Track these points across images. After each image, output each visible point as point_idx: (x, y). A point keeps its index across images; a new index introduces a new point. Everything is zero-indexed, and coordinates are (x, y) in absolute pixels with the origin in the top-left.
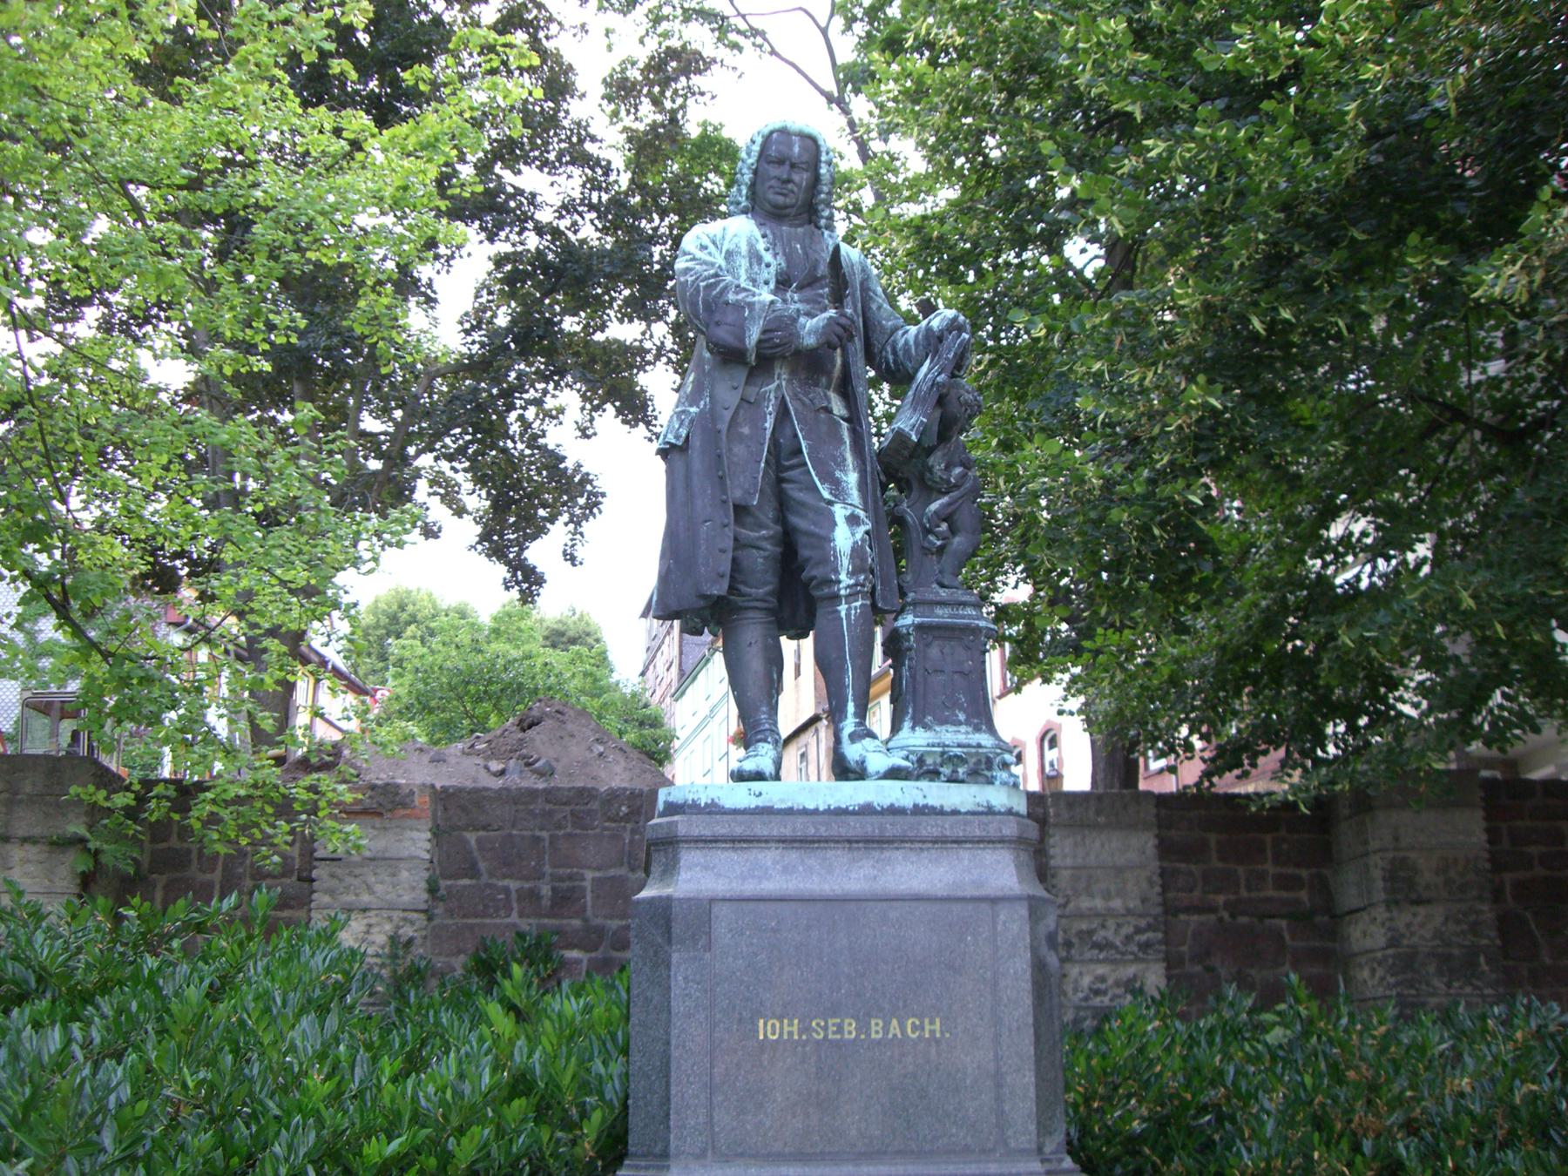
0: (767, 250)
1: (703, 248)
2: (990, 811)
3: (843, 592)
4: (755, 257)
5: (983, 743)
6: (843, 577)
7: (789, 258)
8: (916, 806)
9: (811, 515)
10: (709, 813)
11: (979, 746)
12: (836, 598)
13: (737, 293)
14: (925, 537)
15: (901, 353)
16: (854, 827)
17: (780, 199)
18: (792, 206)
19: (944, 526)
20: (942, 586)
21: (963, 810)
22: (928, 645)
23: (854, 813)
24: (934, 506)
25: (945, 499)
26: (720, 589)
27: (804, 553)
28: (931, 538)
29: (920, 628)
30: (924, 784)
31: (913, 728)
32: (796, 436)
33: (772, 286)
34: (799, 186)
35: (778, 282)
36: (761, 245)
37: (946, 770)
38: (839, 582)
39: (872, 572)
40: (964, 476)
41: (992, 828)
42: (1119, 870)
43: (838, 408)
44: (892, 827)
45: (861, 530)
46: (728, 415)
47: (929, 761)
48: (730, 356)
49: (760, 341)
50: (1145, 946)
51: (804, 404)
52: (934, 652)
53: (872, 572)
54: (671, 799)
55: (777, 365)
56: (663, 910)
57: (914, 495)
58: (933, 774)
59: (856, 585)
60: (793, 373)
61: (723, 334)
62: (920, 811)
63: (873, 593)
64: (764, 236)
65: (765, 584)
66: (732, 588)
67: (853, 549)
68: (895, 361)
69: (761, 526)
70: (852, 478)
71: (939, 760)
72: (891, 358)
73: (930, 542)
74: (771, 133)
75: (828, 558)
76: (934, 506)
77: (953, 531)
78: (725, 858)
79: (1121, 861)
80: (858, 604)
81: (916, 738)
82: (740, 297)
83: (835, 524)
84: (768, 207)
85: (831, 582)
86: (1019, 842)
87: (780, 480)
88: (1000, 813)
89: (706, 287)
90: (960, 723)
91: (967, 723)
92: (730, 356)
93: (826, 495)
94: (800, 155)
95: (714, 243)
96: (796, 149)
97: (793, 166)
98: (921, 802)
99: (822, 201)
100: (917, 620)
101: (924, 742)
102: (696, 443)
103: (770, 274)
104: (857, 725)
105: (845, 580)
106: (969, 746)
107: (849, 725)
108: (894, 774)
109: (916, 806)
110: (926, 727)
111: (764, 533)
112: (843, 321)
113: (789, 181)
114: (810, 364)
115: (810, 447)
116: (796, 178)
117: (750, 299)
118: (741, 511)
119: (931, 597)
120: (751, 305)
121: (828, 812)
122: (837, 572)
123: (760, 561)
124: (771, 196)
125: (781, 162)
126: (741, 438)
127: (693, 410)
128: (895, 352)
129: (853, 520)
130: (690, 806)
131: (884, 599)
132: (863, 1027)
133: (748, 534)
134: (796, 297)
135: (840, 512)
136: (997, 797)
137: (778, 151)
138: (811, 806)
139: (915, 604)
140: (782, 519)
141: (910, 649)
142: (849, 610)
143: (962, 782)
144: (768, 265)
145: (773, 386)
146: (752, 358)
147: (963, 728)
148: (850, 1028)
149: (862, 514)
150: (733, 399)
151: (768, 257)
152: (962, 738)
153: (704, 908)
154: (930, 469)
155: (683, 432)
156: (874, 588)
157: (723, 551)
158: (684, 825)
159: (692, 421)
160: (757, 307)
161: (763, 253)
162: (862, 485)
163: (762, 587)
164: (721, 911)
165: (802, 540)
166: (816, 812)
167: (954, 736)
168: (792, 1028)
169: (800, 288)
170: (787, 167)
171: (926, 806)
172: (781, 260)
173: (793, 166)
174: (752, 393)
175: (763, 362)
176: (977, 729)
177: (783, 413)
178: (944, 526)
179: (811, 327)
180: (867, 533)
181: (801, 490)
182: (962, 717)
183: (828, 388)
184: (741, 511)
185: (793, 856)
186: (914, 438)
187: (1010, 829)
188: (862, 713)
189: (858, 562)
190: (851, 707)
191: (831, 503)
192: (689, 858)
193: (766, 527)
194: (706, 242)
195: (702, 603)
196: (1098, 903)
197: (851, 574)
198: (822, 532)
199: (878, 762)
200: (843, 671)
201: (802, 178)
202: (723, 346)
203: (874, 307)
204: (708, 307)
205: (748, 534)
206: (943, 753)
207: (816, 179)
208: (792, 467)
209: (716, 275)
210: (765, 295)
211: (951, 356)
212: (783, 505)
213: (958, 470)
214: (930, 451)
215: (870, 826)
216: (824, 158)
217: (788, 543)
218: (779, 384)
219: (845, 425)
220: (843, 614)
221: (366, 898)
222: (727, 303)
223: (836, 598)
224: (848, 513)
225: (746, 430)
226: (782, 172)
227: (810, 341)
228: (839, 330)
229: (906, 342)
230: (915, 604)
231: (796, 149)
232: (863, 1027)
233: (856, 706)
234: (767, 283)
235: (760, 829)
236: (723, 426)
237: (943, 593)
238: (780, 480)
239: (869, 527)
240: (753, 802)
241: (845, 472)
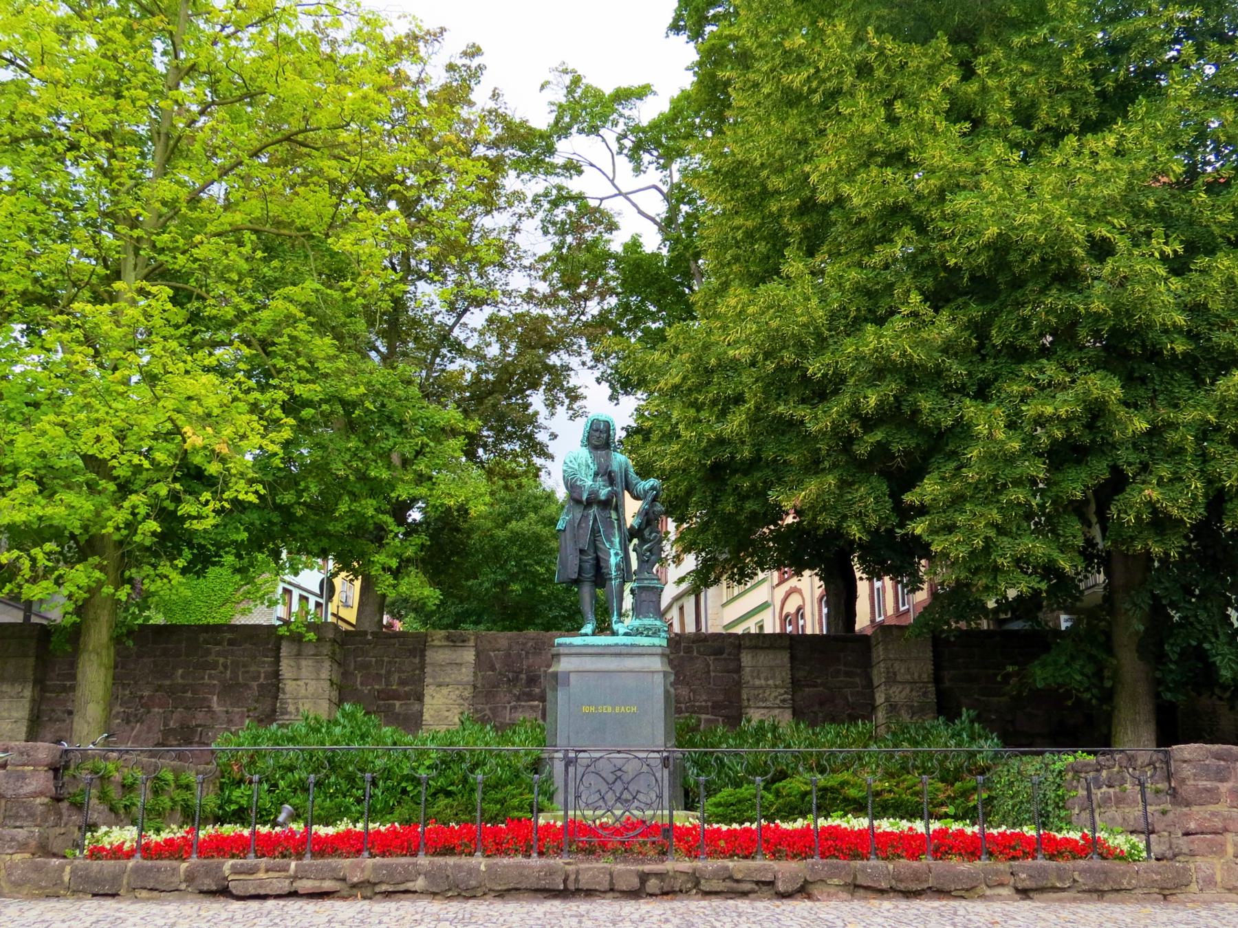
2: (654, 646)
16: (612, 650)
26: (575, 576)
41: (654, 650)
42: (771, 668)
43: (614, 516)
44: (625, 650)
48: (578, 502)
50: (783, 701)
56: (555, 675)
61: (575, 495)
62: (632, 645)
66: (579, 574)
70: (617, 540)
75: (608, 567)
77: (652, 554)
78: (574, 660)
79: (773, 663)
81: (637, 623)
86: (663, 655)
92: (578, 502)
103: (592, 472)
108: (626, 634)
111: (589, 557)
118: (582, 551)
129: (616, 554)
132: (614, 709)
135: (612, 552)
136: (656, 641)
140: (595, 552)
148: (610, 710)
150: (579, 516)
153: (567, 674)
158: (562, 650)
163: (589, 575)
164: (573, 677)
168: (593, 709)
175: (589, 504)
177: (595, 519)
179: (604, 493)
184: (582, 551)
185: (594, 659)
187: (659, 651)
192: (564, 660)
196: (763, 682)
199: (622, 631)
210: (589, 482)
212: (596, 549)
215: (617, 650)
217: (597, 559)
218: (594, 510)
221: (447, 680)
226: (597, 434)
227: (603, 498)
232: (614, 709)
235: (584, 650)
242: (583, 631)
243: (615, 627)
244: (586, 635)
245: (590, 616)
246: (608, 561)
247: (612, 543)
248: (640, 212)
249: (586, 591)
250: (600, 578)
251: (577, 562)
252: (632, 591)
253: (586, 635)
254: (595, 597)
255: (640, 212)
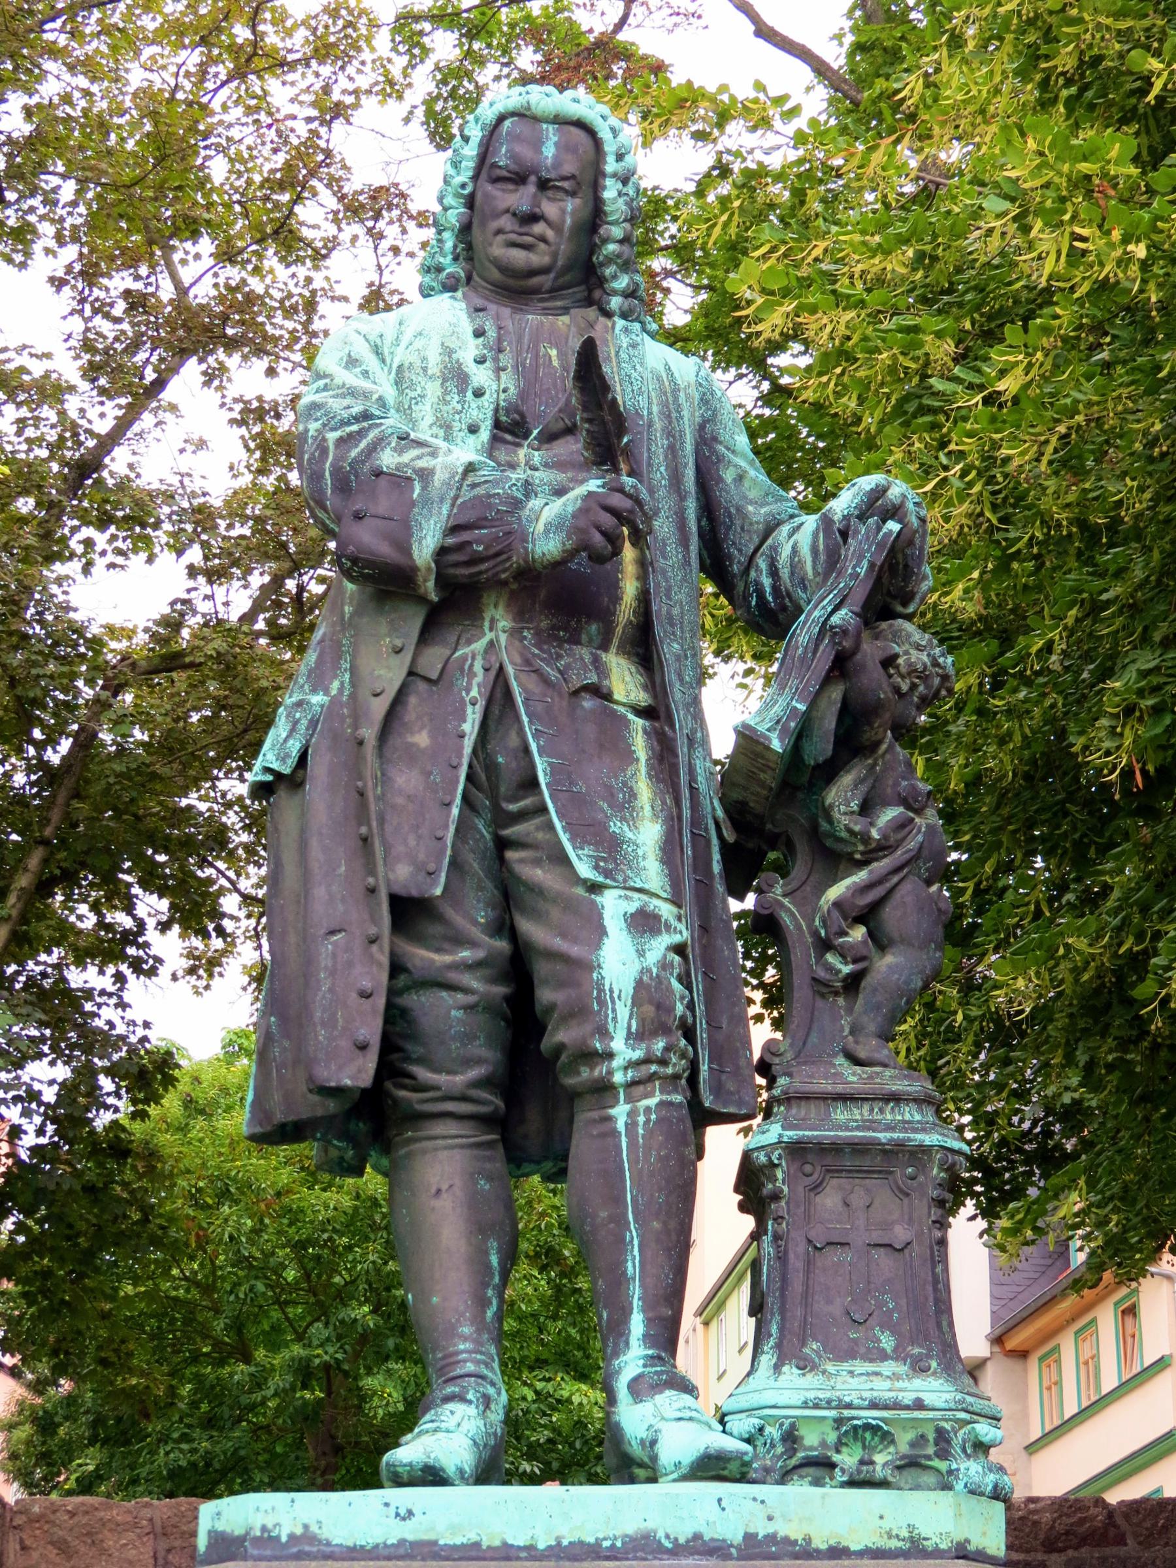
0: (480, 361)
1: (352, 362)
3: (618, 1078)
4: (457, 377)
5: (928, 1399)
6: (618, 1044)
7: (529, 375)
8: (749, 1537)
9: (555, 913)
10: (299, 1556)
11: (919, 1405)
12: (604, 1090)
13: (400, 451)
14: (820, 956)
15: (785, 573)
17: (518, 257)
18: (544, 271)
19: (858, 933)
20: (857, 1062)
21: (854, 1547)
22: (816, 1188)
23: (613, 1555)
24: (835, 892)
25: (861, 876)
26: (358, 1072)
27: (545, 995)
28: (830, 958)
29: (796, 1150)
30: (799, 1491)
31: (777, 1368)
32: (526, 750)
33: (485, 435)
34: (557, 228)
35: (497, 424)
36: (469, 350)
37: (848, 1459)
38: (610, 1055)
39: (689, 1034)
40: (903, 825)
45: (658, 947)
46: (379, 707)
47: (811, 1438)
48: (386, 582)
49: (442, 552)
51: (545, 680)
52: (829, 1200)
53: (689, 1034)
54: (221, 1526)
55: (488, 598)
57: (799, 871)
58: (820, 1466)
59: (647, 1061)
60: (521, 615)
61: (369, 539)
63: (693, 1081)
64: (479, 333)
65: (468, 1062)
67: (639, 985)
68: (776, 589)
69: (459, 940)
70: (646, 834)
71: (832, 1437)
72: (767, 582)
73: (830, 968)
74: (501, 119)
75: (588, 1008)
76: (835, 892)
77: (879, 940)
80: (652, 1102)
81: (787, 1390)
82: (406, 458)
83: (602, 932)
84: (496, 275)
85: (592, 1057)
87: (502, 844)
88: (937, 1554)
89: (340, 441)
90: (883, 1356)
91: (899, 1354)
92: (386, 582)
93: (584, 870)
94: (557, 163)
95: (377, 351)
96: (549, 151)
97: (544, 185)
98: (762, 1529)
99: (609, 260)
100: (791, 1135)
101: (797, 1398)
102: (318, 768)
103: (482, 412)
104: (651, 1360)
105: (623, 1051)
106: (896, 1406)
107: (632, 1360)
108: (711, 1467)
109: (749, 1537)
110: (806, 1365)
111: (461, 958)
112: (617, 500)
113: (533, 218)
114: (566, 598)
115: (554, 770)
116: (550, 209)
117: (421, 464)
118: (409, 912)
119: (824, 1085)
120: (425, 475)
121: (558, 1552)
122: (604, 1033)
123: (456, 1015)
124: (497, 250)
125: (518, 178)
126: (412, 755)
127: (318, 699)
128: (774, 573)
129: (644, 923)
130: (257, 1541)
131: (717, 1089)
133: (424, 957)
134: (537, 457)
135: (614, 906)
137: (512, 156)
138: (519, 1539)
139: (788, 1099)
140: (505, 927)
141: (776, 1196)
142: (632, 1114)
143: (883, 1484)
144: (478, 393)
145: (480, 645)
146: (429, 587)
147: (888, 1367)
149: (666, 910)
151: (481, 376)
152: (882, 1389)
154: (827, 813)
155: (295, 747)
156: (694, 1066)
157: (365, 995)
159: (313, 723)
160: (439, 477)
161: (471, 368)
162: (669, 850)
165: (541, 969)
166: (531, 1552)
167: (866, 1383)
169: (549, 437)
170: (531, 189)
171: (771, 1538)
172: (508, 380)
173: (544, 185)
174: (433, 660)
175: (453, 595)
176: (919, 1368)
178: (858, 933)
180: (679, 949)
181: (537, 862)
182: (887, 1342)
183: (605, 647)
184: (409, 912)
186: (776, 745)
188: (665, 1336)
189: (649, 1010)
190: (637, 1324)
191: (595, 888)
193: (473, 944)
194: (362, 350)
195: (332, 1106)
197: (635, 1038)
198: (575, 950)
199: (680, 1443)
200: (620, 1243)
201: (564, 210)
202: (370, 564)
203: (729, 476)
204: (343, 485)
205: (424, 957)
206: (839, 1422)
207: (596, 215)
208: (522, 816)
209: (366, 416)
210: (467, 450)
211: (862, 570)
212: (509, 898)
213: (889, 814)
214: (829, 771)
216: (611, 166)
217: (518, 969)
218: (494, 638)
219: (638, 723)
220: (621, 1126)
222: (378, 473)
223: (604, 1090)
224: (632, 907)
225: (422, 739)
226: (522, 198)
227: (546, 545)
228: (608, 520)
229: (795, 551)
230: (788, 1099)
231: (549, 151)
233: (649, 1322)
234: (473, 430)
236: (369, 733)
237: (852, 1077)
238: (502, 844)
239: (682, 934)
240: (393, 1532)
241: (632, 820)
242: (409, 1452)
243: (635, 1419)
244: (432, 1476)
245: (468, 1348)
246: (580, 968)
247: (612, 853)
248: (764, 32)
249: (445, 1173)
250: (533, 1091)
251: (377, 978)
252: (752, 1184)
253: (432, 1476)
254: (501, 1229)
255: (764, 32)
